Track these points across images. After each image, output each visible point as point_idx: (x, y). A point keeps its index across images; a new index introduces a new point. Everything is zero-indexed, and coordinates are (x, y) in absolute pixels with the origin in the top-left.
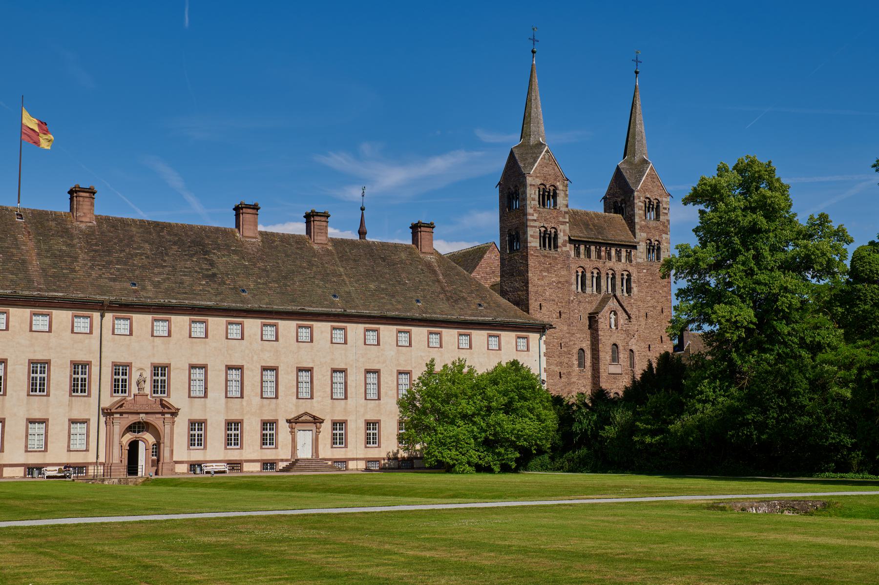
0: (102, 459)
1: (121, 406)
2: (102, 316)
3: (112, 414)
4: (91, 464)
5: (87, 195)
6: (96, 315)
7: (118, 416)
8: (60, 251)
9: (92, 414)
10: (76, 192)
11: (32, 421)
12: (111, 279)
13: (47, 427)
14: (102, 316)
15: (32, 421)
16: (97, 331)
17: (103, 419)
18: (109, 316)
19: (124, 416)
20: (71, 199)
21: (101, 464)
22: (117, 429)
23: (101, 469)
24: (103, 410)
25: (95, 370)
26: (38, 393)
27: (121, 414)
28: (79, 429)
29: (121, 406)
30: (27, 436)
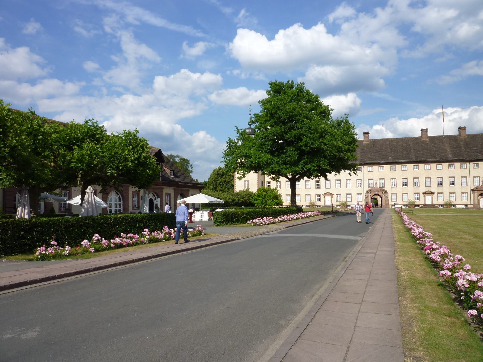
0: (472, 203)
1: (477, 188)
2: (469, 163)
3: (475, 191)
4: (469, 204)
5: (463, 129)
6: (468, 163)
7: (476, 191)
8: (456, 146)
9: (468, 191)
10: (460, 128)
11: (451, 193)
12: (472, 153)
13: (455, 194)
14: (469, 163)
15: (451, 193)
16: (468, 168)
17: (472, 192)
18: (472, 163)
19: (478, 191)
20: (459, 131)
21: (472, 205)
22: (476, 195)
23: (472, 206)
24: (471, 189)
25: (468, 179)
26: (452, 185)
27: (477, 191)
28: (465, 195)
29: (477, 188)
30: (450, 197)
